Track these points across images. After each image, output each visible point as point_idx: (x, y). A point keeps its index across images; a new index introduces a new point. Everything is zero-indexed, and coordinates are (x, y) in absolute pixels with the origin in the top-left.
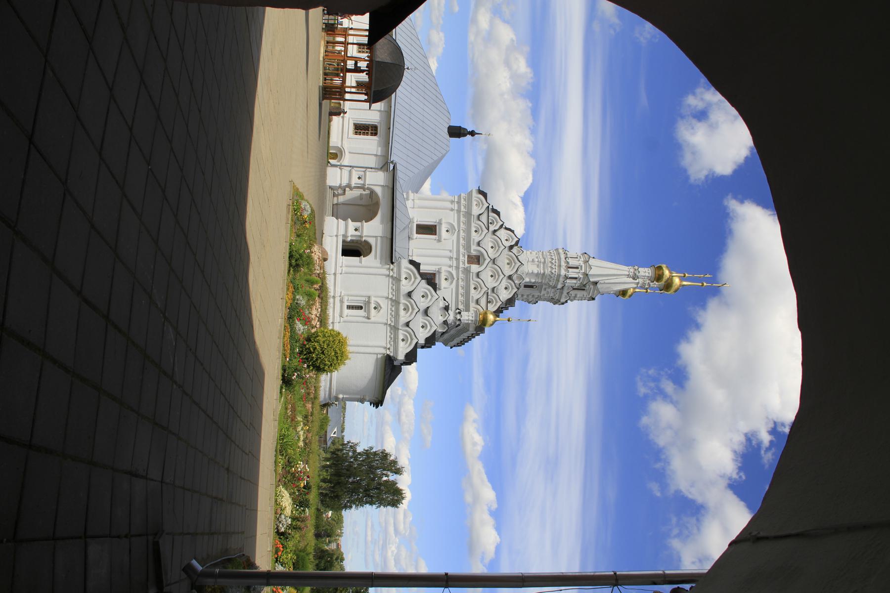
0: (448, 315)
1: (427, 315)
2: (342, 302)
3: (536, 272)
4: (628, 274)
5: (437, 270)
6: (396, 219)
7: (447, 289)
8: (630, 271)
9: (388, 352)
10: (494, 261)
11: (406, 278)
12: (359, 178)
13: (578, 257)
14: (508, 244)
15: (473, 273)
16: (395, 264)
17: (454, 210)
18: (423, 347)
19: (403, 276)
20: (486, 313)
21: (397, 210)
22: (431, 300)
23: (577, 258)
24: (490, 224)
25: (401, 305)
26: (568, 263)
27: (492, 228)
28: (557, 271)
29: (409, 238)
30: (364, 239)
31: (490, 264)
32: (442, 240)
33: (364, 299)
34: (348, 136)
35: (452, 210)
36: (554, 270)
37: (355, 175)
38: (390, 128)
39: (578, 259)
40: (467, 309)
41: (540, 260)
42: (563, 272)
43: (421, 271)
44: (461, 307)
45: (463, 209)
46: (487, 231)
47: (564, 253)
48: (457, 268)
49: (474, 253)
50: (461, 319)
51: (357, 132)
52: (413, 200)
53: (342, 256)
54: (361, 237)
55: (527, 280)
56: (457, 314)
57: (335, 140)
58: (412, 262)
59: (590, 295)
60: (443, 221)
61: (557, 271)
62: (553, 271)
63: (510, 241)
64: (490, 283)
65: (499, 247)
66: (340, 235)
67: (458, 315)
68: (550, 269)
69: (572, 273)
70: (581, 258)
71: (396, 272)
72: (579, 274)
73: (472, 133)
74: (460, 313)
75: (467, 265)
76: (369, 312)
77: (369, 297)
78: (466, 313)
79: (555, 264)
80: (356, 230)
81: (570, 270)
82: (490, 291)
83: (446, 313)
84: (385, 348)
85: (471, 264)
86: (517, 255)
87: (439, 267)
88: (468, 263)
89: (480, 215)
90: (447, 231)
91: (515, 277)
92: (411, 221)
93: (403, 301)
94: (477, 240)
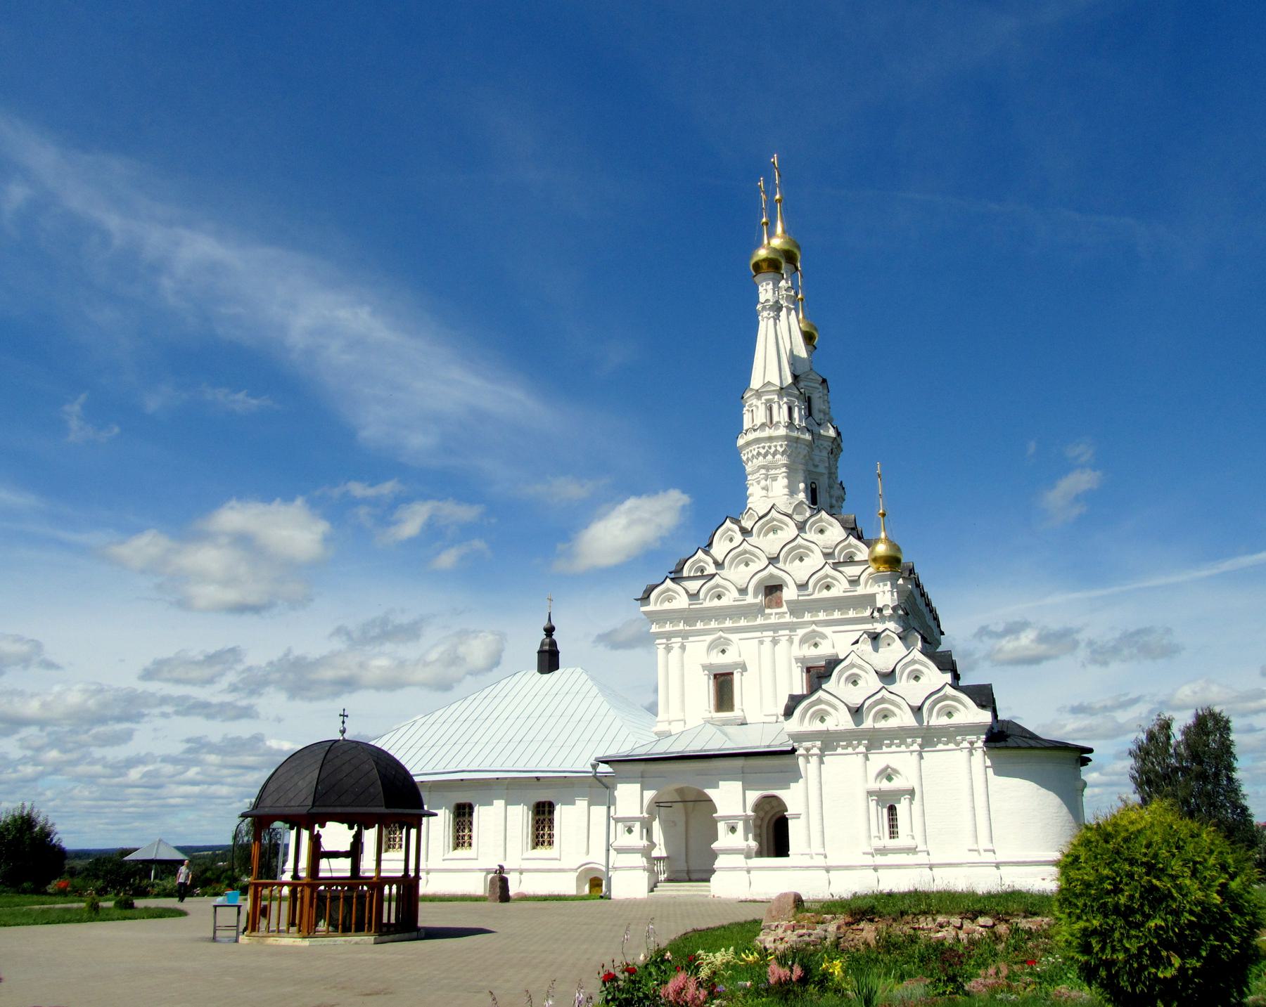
0: (887, 632)
1: (894, 671)
2: (883, 851)
3: (785, 481)
4: (772, 319)
5: (799, 664)
6: (705, 751)
7: (837, 642)
8: (766, 317)
9: (980, 744)
10: (773, 560)
11: (822, 720)
12: (630, 831)
13: (750, 409)
14: (738, 537)
15: (798, 596)
16: (796, 745)
17: (683, 643)
18: (956, 677)
19: (818, 726)
20: (875, 560)
21: (688, 749)
22: (860, 667)
23: (752, 410)
24: (705, 573)
25: (878, 725)
26: (763, 425)
27: (711, 569)
28: (780, 443)
29: (742, 724)
30: (750, 813)
31: (780, 565)
32: (738, 659)
33: (873, 805)
34: (556, 859)
35: (683, 648)
36: (779, 448)
37: (624, 840)
38: (537, 778)
39: (754, 408)
40: (871, 598)
41: (762, 476)
42: (782, 431)
43: (805, 693)
44: (868, 613)
45: (681, 626)
46: (717, 576)
47: (746, 434)
48: (792, 627)
49: (760, 599)
50: (891, 606)
51: (549, 842)
52: (670, 723)
53: (788, 856)
54: (746, 820)
55: (802, 496)
56: (884, 615)
57: (567, 885)
58: (789, 713)
59: (817, 385)
60: (707, 661)
61: (780, 443)
62: (781, 450)
63: (733, 534)
64: (815, 560)
65: (745, 552)
66: (747, 864)
67: (884, 612)
68: (778, 456)
69: (781, 415)
70: (752, 404)
71: (810, 743)
72: (781, 403)
73: (549, 631)
74: (880, 610)
75: (784, 609)
76: (899, 794)
77: (870, 793)
78: (878, 597)
79: (766, 448)
80: (733, 829)
81: (775, 419)
82: (831, 561)
83: (882, 635)
84: (971, 754)
85: (781, 601)
86: (758, 519)
87: (793, 661)
89: (687, 592)
90: (723, 651)
91: (799, 518)
92: (709, 721)
93: (868, 723)
94: (735, 594)
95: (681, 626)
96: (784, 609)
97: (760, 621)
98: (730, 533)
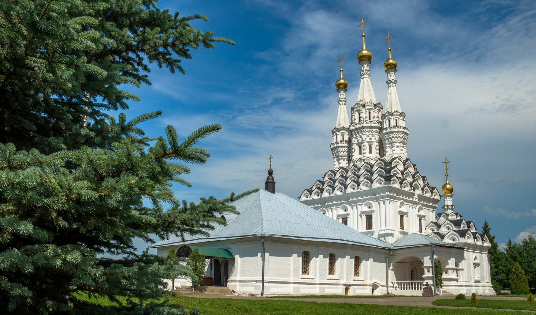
48: (416, 203)
73: (270, 173)
88: (415, 196)
96: (416, 197)
97: (411, 199)
98: (397, 163)
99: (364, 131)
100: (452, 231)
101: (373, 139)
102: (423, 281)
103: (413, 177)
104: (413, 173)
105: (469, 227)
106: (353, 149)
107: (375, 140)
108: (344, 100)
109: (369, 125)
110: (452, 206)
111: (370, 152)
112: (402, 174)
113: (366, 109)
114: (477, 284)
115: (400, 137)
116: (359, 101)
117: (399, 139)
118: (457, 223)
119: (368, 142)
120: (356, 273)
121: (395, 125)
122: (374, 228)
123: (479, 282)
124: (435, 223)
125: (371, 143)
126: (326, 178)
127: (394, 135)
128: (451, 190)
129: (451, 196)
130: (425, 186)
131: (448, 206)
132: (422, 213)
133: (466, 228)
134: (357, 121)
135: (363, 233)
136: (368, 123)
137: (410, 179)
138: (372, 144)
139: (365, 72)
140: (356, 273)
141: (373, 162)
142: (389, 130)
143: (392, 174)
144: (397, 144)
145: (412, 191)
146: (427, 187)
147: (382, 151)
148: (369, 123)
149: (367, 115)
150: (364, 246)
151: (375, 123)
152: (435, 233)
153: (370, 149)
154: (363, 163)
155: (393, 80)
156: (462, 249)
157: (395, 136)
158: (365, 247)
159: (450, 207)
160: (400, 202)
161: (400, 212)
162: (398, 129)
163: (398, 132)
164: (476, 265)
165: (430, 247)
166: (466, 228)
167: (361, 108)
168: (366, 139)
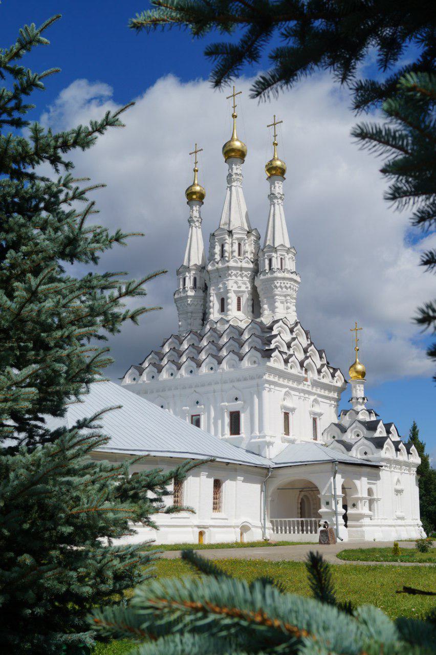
45: (276, 379)
52: (271, 437)
95: (276, 379)
96: (309, 383)
97: (301, 387)
98: (280, 328)
99: (230, 275)
100: (362, 440)
101: (243, 288)
102: (319, 519)
103: (305, 351)
104: (305, 345)
105: (388, 432)
106: (210, 301)
107: (247, 290)
108: (198, 221)
109: (239, 265)
110: (364, 399)
111: (239, 309)
112: (289, 347)
113: (234, 238)
114: (400, 522)
115: (286, 287)
116: (224, 225)
117: (284, 289)
118: (372, 426)
119: (235, 292)
120: (216, 507)
121: (280, 267)
122: (242, 433)
123: (402, 518)
124: (338, 425)
125: (240, 294)
126: (166, 349)
127: (277, 283)
128: (363, 374)
129: (363, 383)
130: (323, 366)
131: (358, 399)
132: (317, 409)
133: (385, 435)
134: (218, 257)
135: (227, 440)
136: (237, 262)
137: (301, 356)
138: (242, 296)
139: (234, 176)
140: (216, 507)
141: (243, 325)
142: (269, 276)
143: (272, 346)
144: (281, 298)
145: (304, 375)
146: (325, 368)
147: (256, 307)
148: (239, 261)
149: (236, 247)
150: (229, 463)
151: (247, 262)
152: (338, 441)
153: (238, 303)
154: (228, 326)
155: (279, 193)
156: (377, 467)
157: (278, 285)
158: (230, 465)
159: (361, 400)
160: (284, 390)
161: (284, 407)
162: (283, 274)
163: (284, 279)
164: (399, 492)
165: (330, 465)
166: (385, 435)
167: (227, 237)
168: (232, 287)
